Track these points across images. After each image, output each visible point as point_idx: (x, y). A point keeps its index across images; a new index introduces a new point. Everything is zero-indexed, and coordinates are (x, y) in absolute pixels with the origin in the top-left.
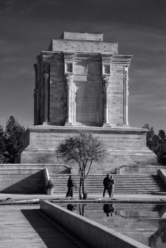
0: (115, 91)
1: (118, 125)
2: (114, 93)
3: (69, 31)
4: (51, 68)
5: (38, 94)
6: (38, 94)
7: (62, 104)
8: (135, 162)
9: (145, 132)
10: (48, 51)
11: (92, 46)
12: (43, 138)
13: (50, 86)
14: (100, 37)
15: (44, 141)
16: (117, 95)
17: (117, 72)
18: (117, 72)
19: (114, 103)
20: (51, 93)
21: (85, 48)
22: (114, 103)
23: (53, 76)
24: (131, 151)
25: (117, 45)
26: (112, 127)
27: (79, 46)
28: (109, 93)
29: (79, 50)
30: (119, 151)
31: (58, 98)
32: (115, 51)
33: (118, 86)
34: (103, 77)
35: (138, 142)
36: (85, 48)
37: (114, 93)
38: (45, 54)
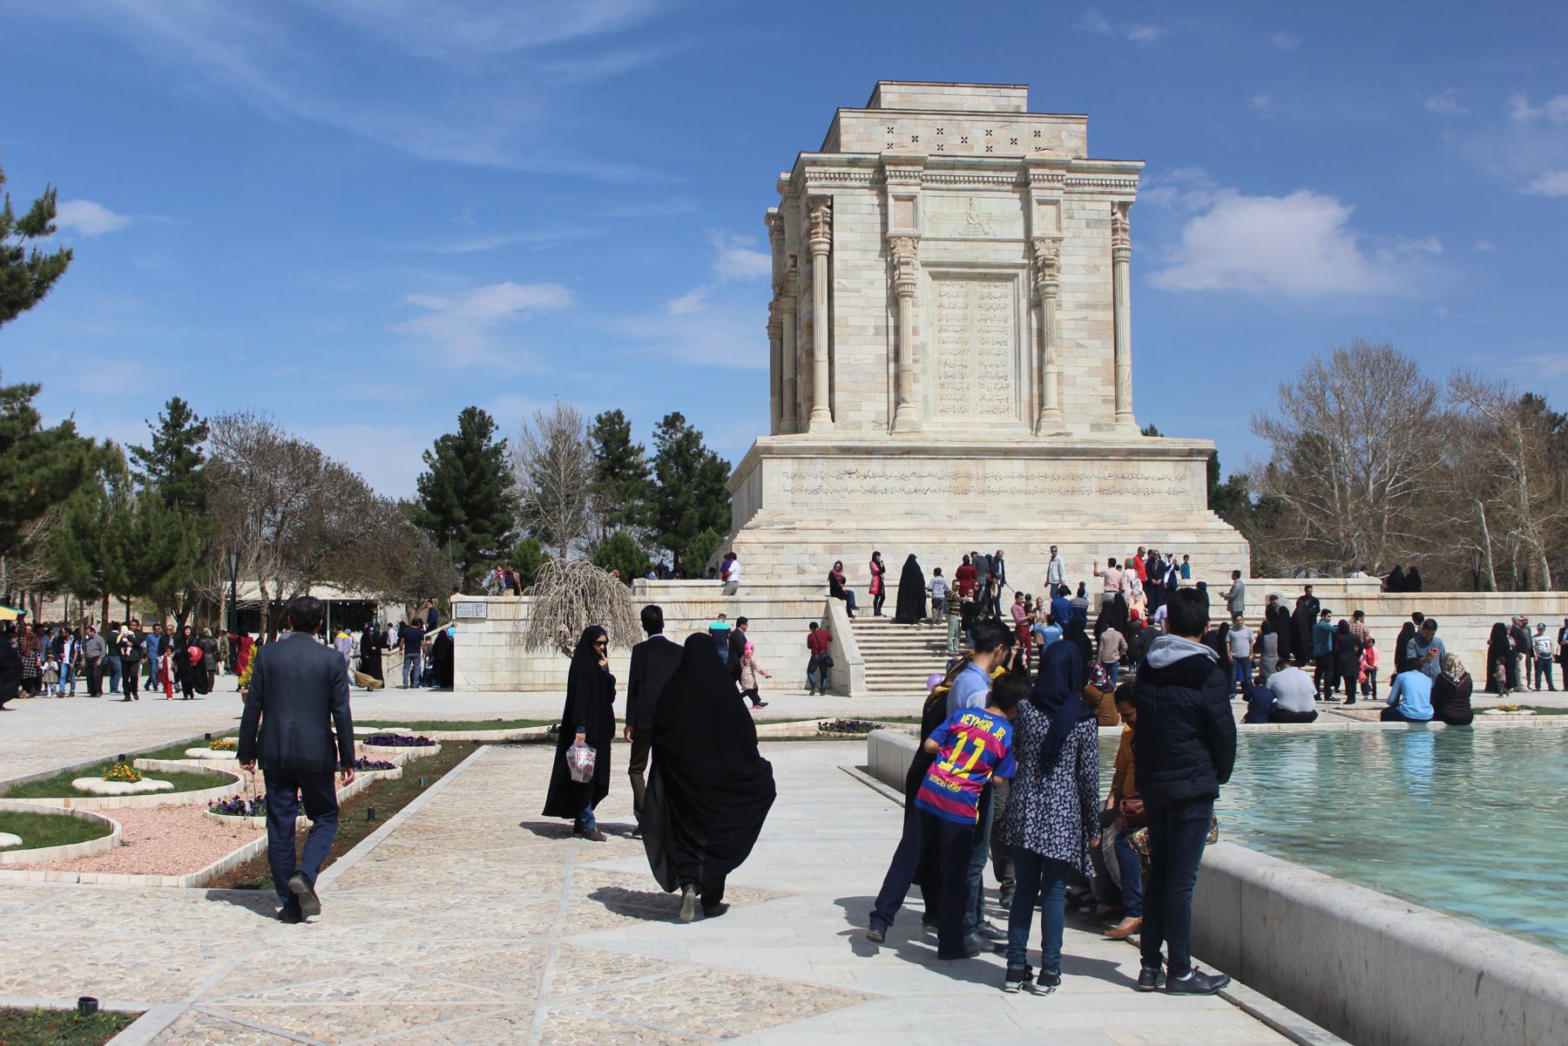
0: (1083, 297)
1: (1096, 427)
2: (1079, 306)
3: (901, 82)
5: (787, 320)
6: (787, 320)
9: (1200, 452)
10: (822, 151)
11: (989, 133)
12: (811, 483)
13: (836, 286)
14: (1015, 102)
15: (816, 491)
16: (1091, 314)
17: (1088, 226)
18: (1088, 226)
19: (1079, 345)
20: (837, 312)
21: (964, 140)
22: (1079, 345)
24: (1152, 526)
25: (1083, 128)
26: (1075, 437)
27: (940, 131)
28: (1059, 306)
29: (940, 148)
30: (1104, 525)
33: (1095, 279)
34: (1038, 245)
35: (1176, 493)
36: (964, 140)
37: (1079, 306)
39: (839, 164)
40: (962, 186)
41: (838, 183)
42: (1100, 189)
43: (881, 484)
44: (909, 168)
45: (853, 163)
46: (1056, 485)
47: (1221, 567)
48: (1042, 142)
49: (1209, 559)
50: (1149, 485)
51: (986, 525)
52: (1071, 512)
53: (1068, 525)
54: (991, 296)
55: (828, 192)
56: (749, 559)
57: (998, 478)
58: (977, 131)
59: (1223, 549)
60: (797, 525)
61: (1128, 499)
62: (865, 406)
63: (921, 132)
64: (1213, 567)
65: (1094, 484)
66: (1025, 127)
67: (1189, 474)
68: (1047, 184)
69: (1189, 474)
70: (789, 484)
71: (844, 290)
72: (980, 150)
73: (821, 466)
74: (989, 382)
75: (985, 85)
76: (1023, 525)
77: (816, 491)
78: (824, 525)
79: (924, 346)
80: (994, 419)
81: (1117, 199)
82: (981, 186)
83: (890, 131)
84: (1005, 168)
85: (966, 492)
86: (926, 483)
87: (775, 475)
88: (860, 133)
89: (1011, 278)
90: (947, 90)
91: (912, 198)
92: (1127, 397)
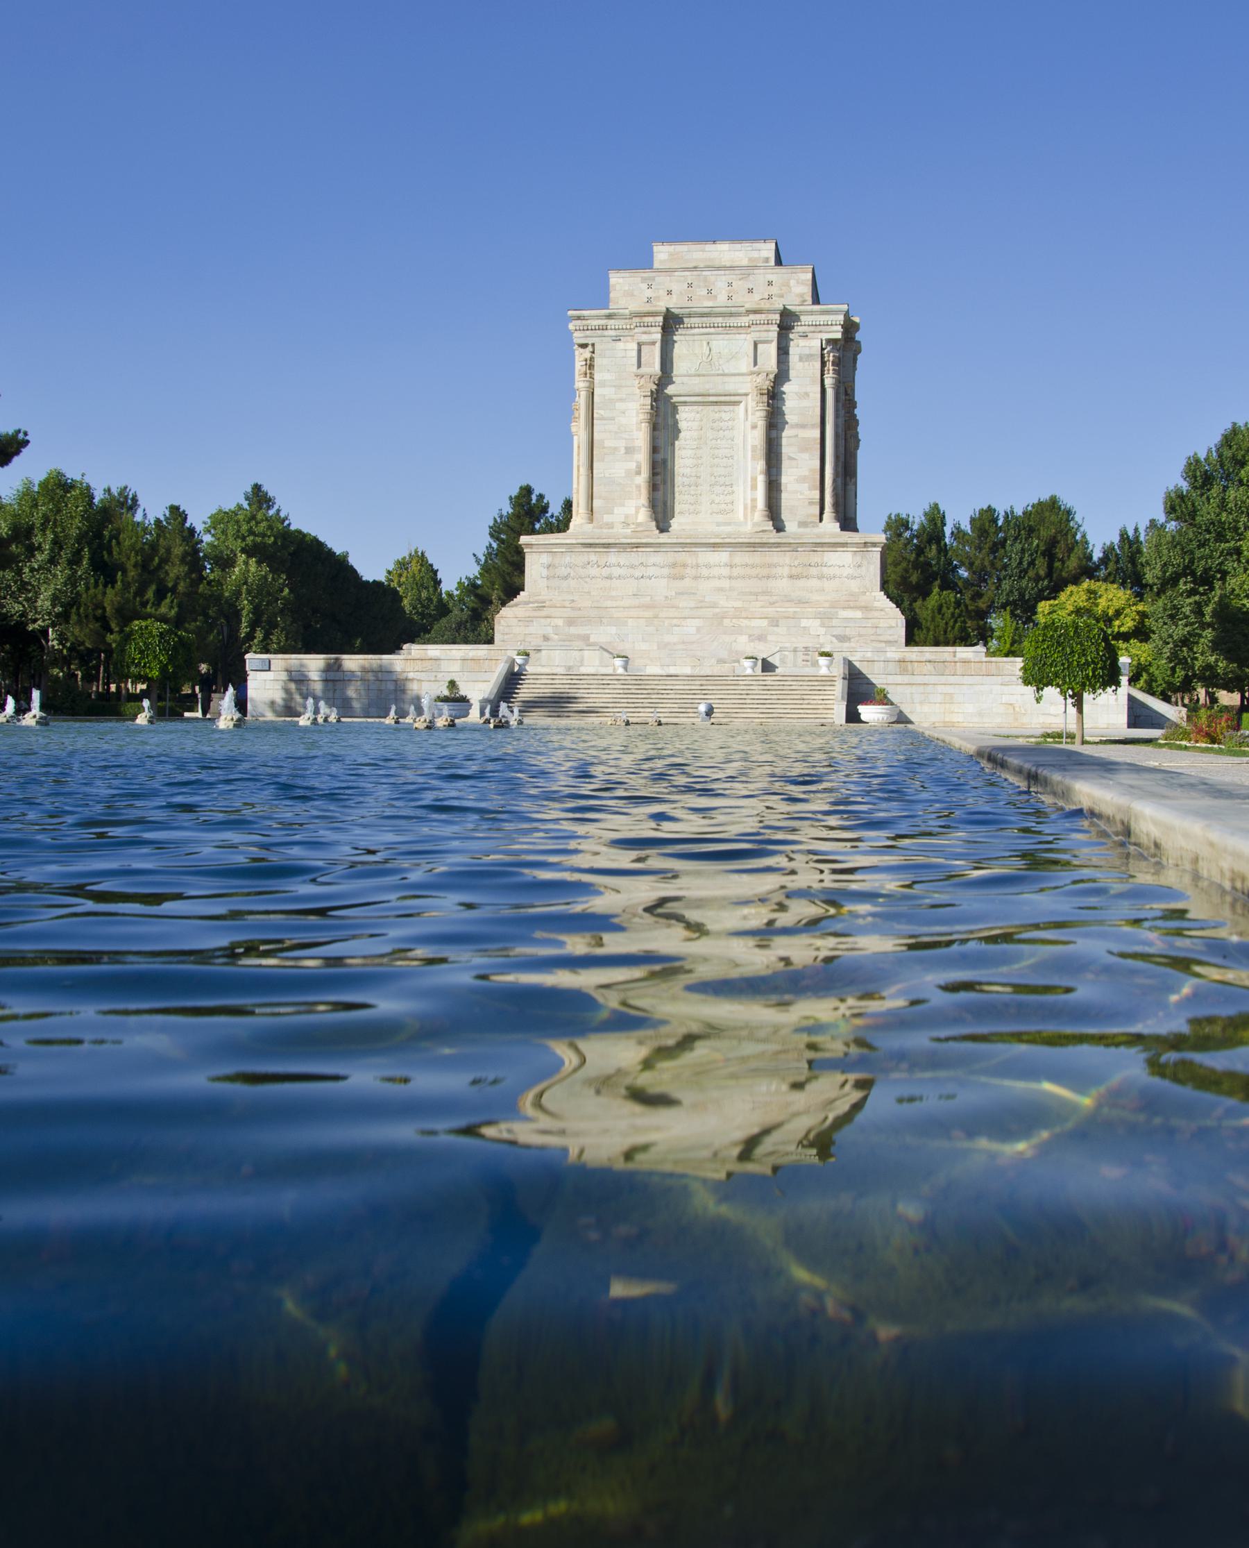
1: (803, 524)
4: (597, 362)
7: (633, 466)
8: (834, 640)
9: (874, 544)
11: (730, 285)
12: (563, 571)
15: (566, 578)
18: (801, 359)
21: (710, 292)
22: (791, 458)
23: (603, 384)
27: (690, 285)
29: (690, 299)
31: (616, 449)
32: (802, 295)
33: (805, 403)
36: (710, 292)
38: (579, 318)
40: (696, 331)
41: (599, 332)
42: (812, 329)
43: (616, 571)
44: (651, 319)
45: (609, 317)
46: (754, 572)
47: (881, 638)
48: (774, 290)
49: (871, 631)
50: (831, 571)
51: (692, 604)
52: (765, 593)
53: (759, 604)
54: (721, 420)
55: (590, 341)
56: (507, 630)
57: (708, 566)
58: (720, 283)
59: (882, 624)
60: (547, 604)
61: (814, 583)
62: (616, 511)
63: (675, 287)
64: (873, 638)
65: (785, 571)
66: (761, 277)
67: (865, 563)
68: (765, 327)
69: (865, 563)
70: (545, 572)
71: (602, 419)
72: (722, 299)
73: (567, 559)
74: (718, 489)
76: (722, 603)
77: (566, 578)
78: (567, 604)
79: (665, 462)
80: (720, 518)
81: (826, 336)
82: (712, 330)
83: (650, 287)
84: (731, 315)
85: (682, 578)
86: (651, 571)
88: (627, 289)
89: (737, 403)
90: (709, 247)
91: (653, 343)
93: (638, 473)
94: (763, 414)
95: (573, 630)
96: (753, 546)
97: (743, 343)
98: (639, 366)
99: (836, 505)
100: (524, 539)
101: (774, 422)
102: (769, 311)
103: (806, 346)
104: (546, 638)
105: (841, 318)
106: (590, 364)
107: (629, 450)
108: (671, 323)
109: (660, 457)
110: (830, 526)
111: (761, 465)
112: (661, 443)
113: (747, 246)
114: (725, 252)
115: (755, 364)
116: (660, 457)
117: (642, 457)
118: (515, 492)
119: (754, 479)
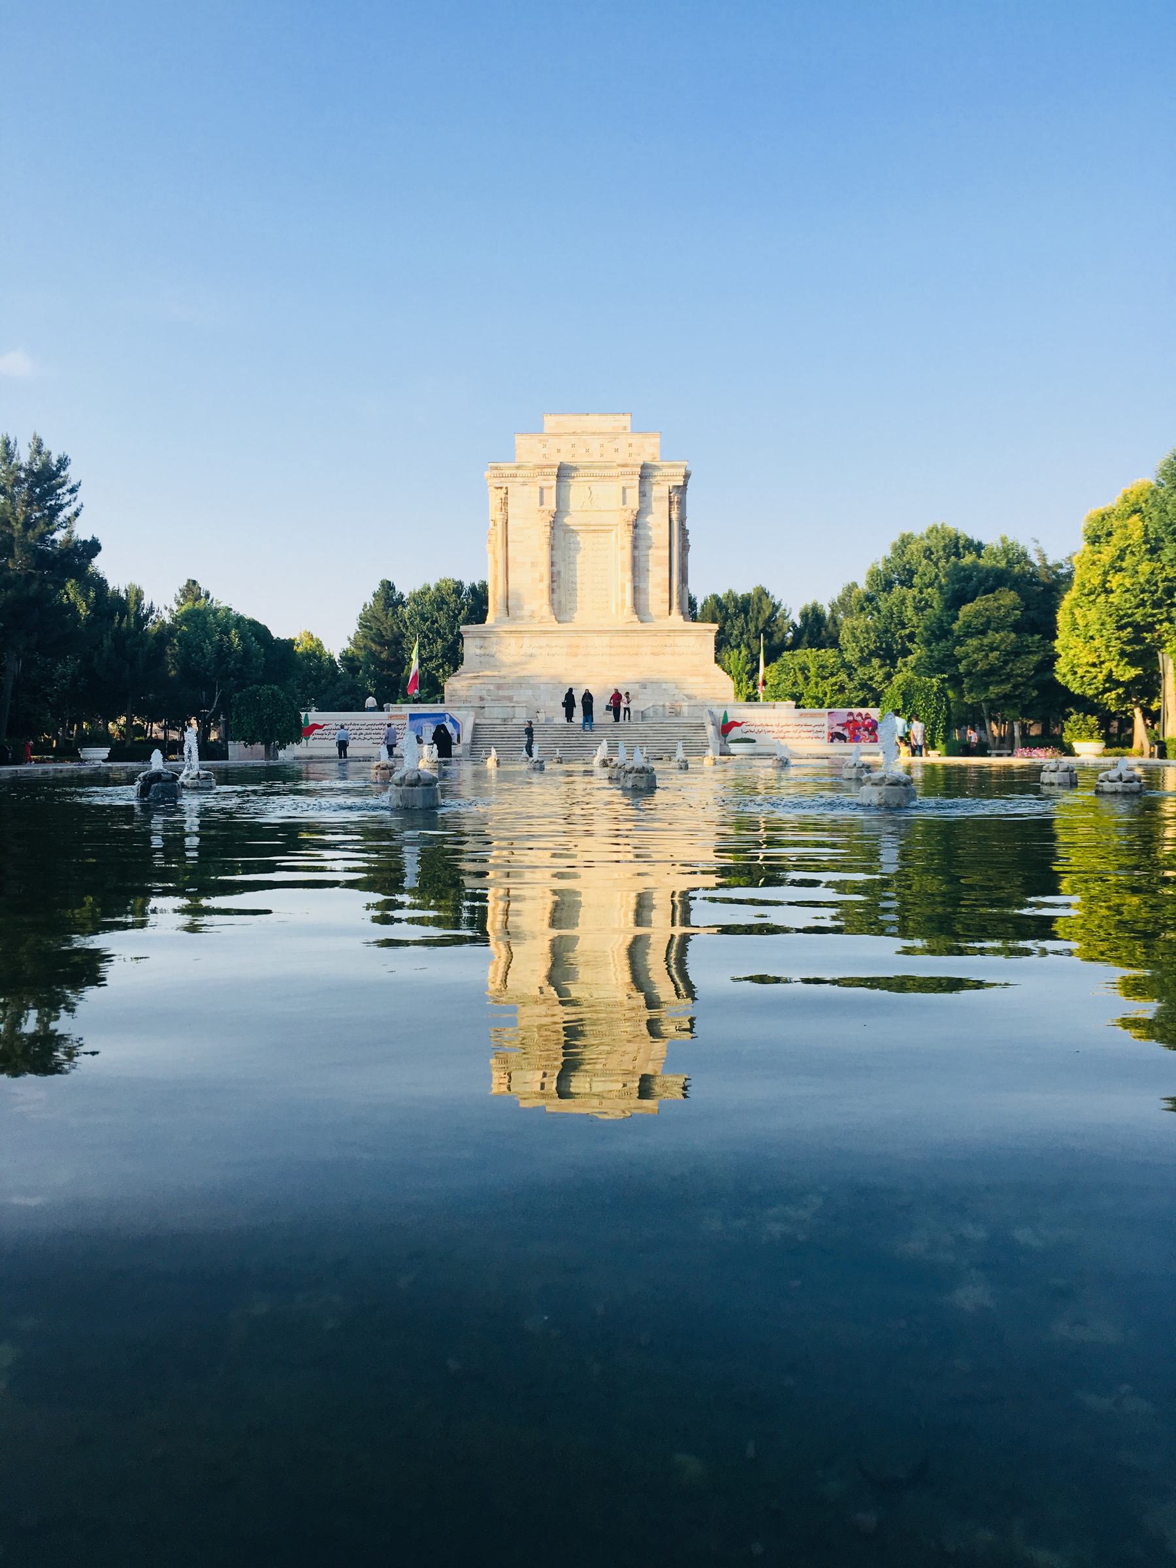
9: (710, 631)
11: (602, 446)
21: (587, 451)
25: (658, 440)
27: (573, 446)
29: (573, 456)
36: (587, 451)
38: (496, 468)
39: (510, 468)
44: (549, 470)
45: (518, 468)
72: (596, 457)
75: (605, 414)
79: (559, 572)
83: (545, 446)
84: (606, 467)
85: (576, 655)
87: (470, 649)
88: (530, 450)
91: (551, 488)
92: (675, 600)
93: (541, 581)
94: (630, 539)
95: (501, 693)
96: (626, 632)
97: (615, 488)
98: (542, 503)
99: (680, 603)
100: (463, 628)
101: (638, 542)
102: (633, 466)
103: (660, 491)
104: (482, 699)
105: (682, 471)
106: (505, 502)
107: (533, 564)
108: (563, 473)
109: (555, 569)
110: (677, 619)
111: (629, 575)
112: (555, 559)
113: (610, 417)
114: (594, 422)
115: (624, 503)
116: (555, 569)
117: (544, 569)
118: (376, 588)
119: (623, 586)
